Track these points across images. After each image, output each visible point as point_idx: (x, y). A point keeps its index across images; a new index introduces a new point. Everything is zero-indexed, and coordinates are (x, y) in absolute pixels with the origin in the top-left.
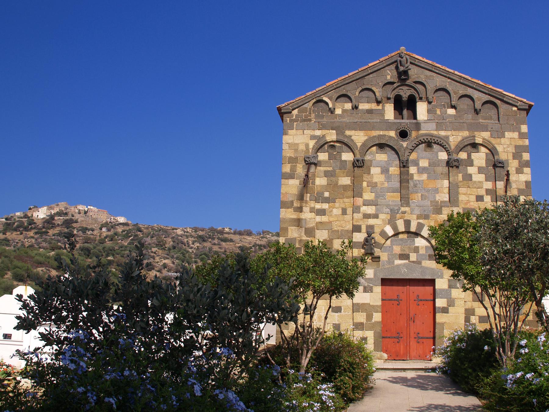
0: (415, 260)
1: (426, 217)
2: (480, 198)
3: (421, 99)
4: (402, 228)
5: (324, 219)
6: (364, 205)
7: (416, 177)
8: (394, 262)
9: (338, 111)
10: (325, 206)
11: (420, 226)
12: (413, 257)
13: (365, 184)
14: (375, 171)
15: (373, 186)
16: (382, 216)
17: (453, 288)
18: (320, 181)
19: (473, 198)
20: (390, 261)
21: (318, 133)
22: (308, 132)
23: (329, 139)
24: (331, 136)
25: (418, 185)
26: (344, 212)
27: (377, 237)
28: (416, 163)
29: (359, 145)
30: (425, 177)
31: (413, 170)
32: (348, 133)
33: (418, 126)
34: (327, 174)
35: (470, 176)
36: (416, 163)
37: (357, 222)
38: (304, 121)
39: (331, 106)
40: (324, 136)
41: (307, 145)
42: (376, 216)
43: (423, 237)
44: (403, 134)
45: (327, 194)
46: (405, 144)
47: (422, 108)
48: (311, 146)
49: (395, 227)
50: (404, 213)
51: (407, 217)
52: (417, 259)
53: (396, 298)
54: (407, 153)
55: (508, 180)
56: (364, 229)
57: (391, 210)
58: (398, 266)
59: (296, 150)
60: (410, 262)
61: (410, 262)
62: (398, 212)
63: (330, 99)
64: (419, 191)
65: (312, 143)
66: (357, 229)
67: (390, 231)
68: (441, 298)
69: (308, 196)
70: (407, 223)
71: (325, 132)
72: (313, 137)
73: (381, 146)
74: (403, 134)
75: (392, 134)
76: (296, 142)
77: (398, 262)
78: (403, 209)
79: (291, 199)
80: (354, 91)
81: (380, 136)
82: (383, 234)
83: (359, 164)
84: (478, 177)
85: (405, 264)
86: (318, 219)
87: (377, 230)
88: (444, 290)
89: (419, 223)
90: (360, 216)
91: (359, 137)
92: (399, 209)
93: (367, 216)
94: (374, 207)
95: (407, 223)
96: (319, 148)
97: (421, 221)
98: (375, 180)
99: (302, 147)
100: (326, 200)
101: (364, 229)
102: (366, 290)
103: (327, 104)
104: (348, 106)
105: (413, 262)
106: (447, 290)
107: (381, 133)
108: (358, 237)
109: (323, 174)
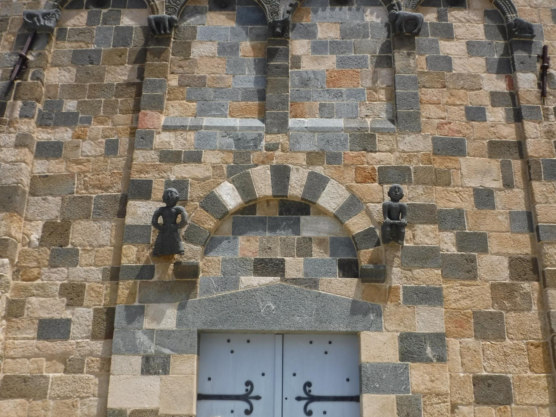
0: (301, 276)
1: (334, 159)
2: (475, 114)
4: (264, 187)
5: (54, 167)
6: (166, 128)
8: (237, 281)
10: (64, 134)
11: (316, 184)
12: (295, 266)
16: (211, 158)
17: (414, 361)
19: (457, 114)
20: (228, 280)
25: (313, 82)
26: (111, 148)
27: (192, 213)
30: (330, 62)
31: (299, 46)
34: (78, 58)
35: (448, 60)
36: (309, 33)
37: (140, 172)
42: (195, 157)
43: (322, 212)
45: (70, 105)
49: (245, 187)
50: (271, 148)
51: (278, 157)
52: (306, 274)
53: (241, 390)
55: (544, 68)
56: (158, 190)
57: (238, 140)
58: (251, 293)
60: (286, 280)
61: (286, 280)
62: (256, 146)
64: (315, 95)
66: (142, 190)
67: (230, 196)
68: (377, 391)
70: (281, 175)
77: (251, 281)
78: (268, 139)
82: (212, 203)
84: (465, 64)
85: (268, 288)
86: (42, 167)
87: (195, 192)
88: (384, 367)
89: (313, 176)
90: (152, 156)
92: (259, 138)
93: (170, 157)
94: (192, 136)
95: (281, 175)
97: (319, 169)
98: (202, 71)
100: (69, 120)
101: (158, 190)
102: (153, 366)
105: (295, 281)
106: (395, 367)
108: (140, 212)
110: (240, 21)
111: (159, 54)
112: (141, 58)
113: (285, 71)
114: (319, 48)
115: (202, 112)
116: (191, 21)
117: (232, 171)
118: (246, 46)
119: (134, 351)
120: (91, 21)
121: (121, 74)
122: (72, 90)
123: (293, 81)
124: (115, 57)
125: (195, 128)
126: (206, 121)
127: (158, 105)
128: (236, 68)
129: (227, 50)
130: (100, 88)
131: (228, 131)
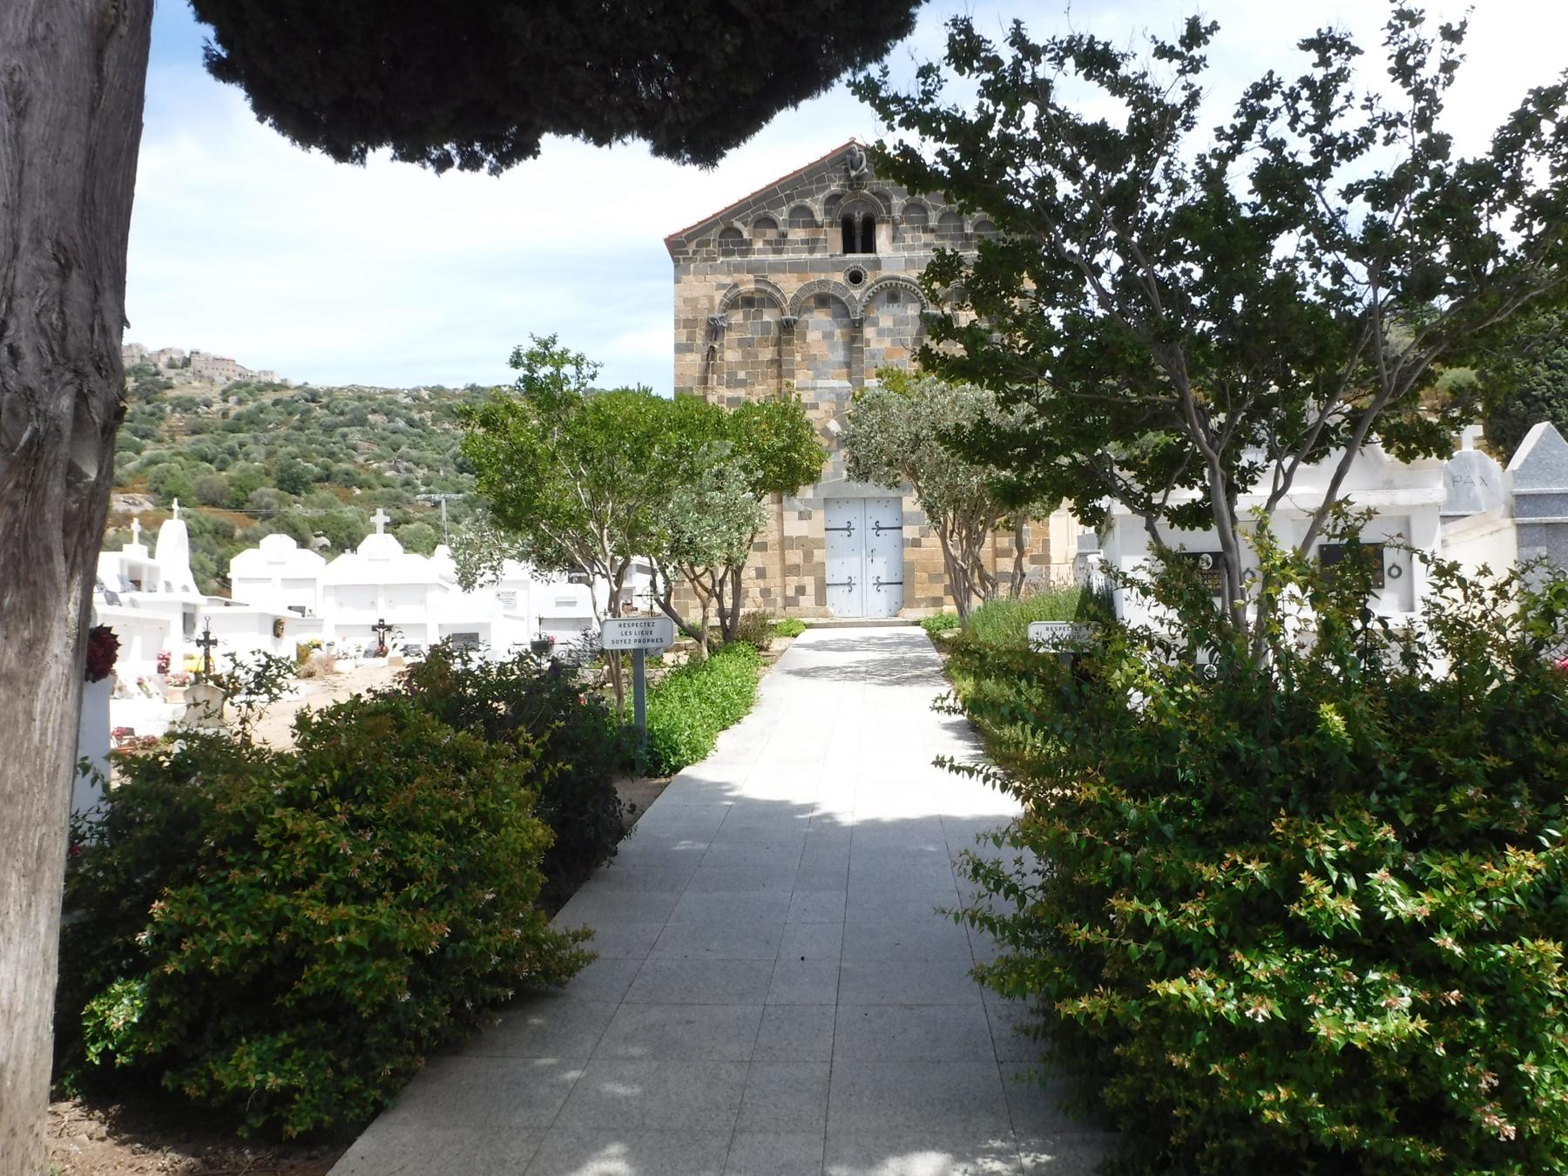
3: (883, 221)
7: (874, 345)
9: (759, 245)
13: (798, 357)
14: (813, 336)
15: (810, 360)
16: (824, 406)
18: (731, 356)
21: (728, 280)
22: (714, 279)
23: (743, 288)
24: (748, 285)
28: (875, 323)
29: (789, 296)
30: (887, 343)
31: (869, 332)
32: (772, 278)
33: (877, 265)
38: (706, 260)
39: (746, 235)
40: (736, 286)
41: (711, 299)
44: (856, 278)
45: (742, 375)
46: (857, 293)
47: (883, 236)
48: (717, 301)
54: (860, 308)
59: (695, 308)
63: (745, 224)
65: (719, 297)
69: (713, 379)
71: (737, 277)
72: (720, 286)
73: (823, 301)
74: (856, 278)
75: (840, 278)
76: (695, 294)
79: (689, 384)
80: (782, 215)
81: (820, 282)
83: (787, 327)
91: (789, 285)
94: (812, 393)
96: (732, 305)
99: (704, 303)
100: (742, 383)
102: (803, 516)
103: (740, 233)
104: (771, 234)
107: (823, 277)
109: (735, 344)
110: (835, 316)
111: (789, 342)
112: (778, 343)
113: (861, 350)
114: (881, 333)
115: (816, 377)
116: (805, 317)
117: (835, 413)
118: (838, 332)
119: (794, 509)
120: (746, 318)
121: (767, 354)
122: (742, 365)
123: (866, 355)
124: (763, 342)
125: (814, 389)
126: (820, 383)
127: (792, 374)
128: (833, 348)
129: (828, 336)
130: (756, 364)
131: (832, 389)
